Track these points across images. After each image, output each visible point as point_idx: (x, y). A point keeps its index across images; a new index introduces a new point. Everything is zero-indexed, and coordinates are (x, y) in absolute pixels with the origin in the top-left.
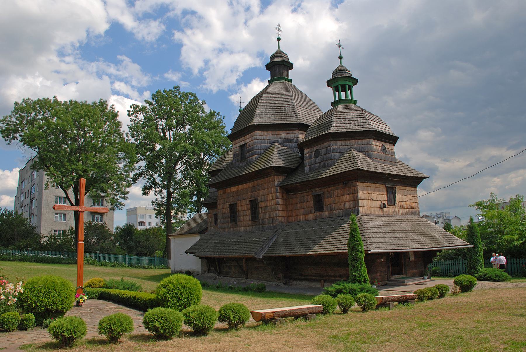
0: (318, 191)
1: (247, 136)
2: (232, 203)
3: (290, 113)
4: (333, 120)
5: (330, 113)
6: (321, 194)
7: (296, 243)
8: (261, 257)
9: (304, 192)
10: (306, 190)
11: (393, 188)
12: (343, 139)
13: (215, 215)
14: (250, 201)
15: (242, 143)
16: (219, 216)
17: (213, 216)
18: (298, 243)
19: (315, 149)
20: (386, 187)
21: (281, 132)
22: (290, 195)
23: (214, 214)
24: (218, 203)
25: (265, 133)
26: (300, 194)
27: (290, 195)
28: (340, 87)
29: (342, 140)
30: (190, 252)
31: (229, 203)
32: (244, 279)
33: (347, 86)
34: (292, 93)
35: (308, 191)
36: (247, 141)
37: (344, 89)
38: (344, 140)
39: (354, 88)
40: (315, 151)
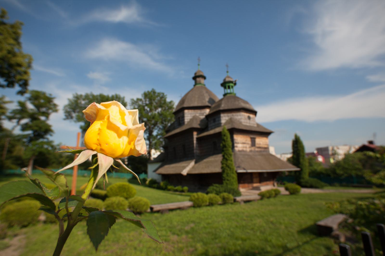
5: (221, 100)
34: (204, 91)
37: (229, 87)
39: (235, 88)
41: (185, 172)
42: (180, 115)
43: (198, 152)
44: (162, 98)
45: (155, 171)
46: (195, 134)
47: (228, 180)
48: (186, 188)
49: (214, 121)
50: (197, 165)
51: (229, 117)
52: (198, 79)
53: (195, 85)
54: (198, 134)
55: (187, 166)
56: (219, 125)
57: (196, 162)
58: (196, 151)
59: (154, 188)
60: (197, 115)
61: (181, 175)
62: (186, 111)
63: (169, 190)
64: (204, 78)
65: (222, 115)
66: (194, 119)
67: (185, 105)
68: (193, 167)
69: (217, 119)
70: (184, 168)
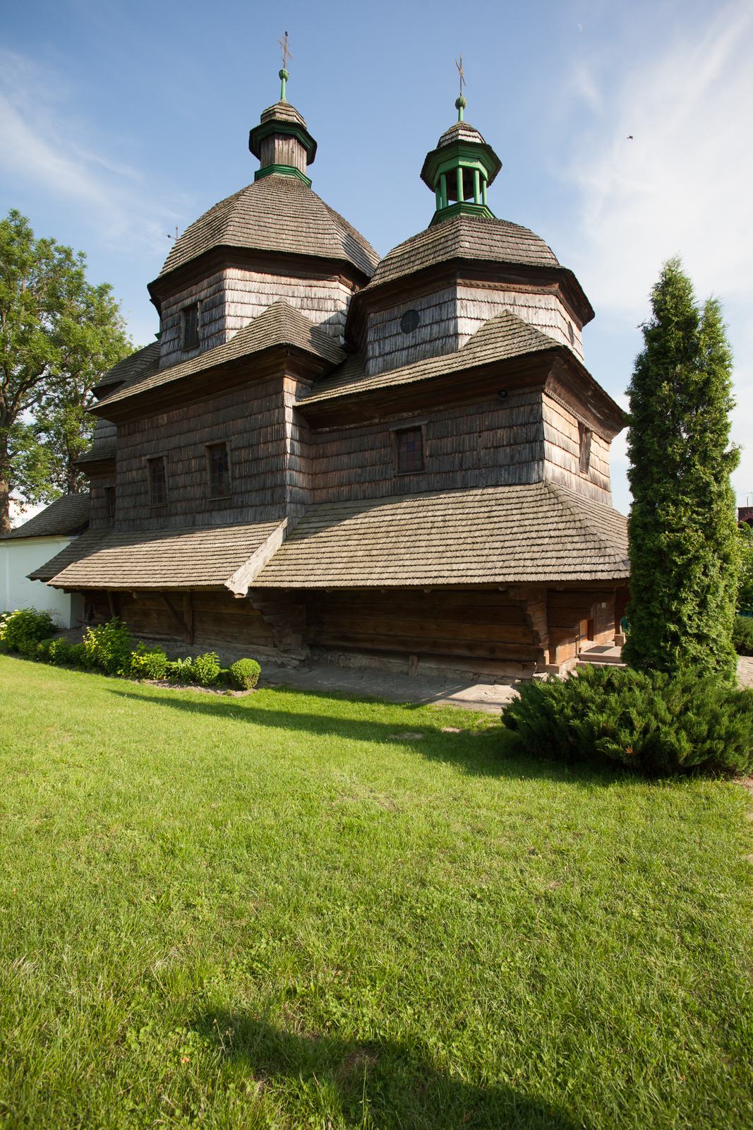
0: (407, 420)
1: (205, 283)
2: (155, 456)
3: (320, 236)
4: (462, 232)
6: (419, 429)
7: (351, 554)
8: (245, 591)
9: (365, 423)
10: (375, 418)
11: (587, 430)
12: (486, 283)
13: (110, 491)
14: (207, 447)
15: (188, 302)
16: (118, 491)
17: (103, 493)
18: (360, 553)
19: (403, 309)
20: (580, 423)
21: (294, 281)
22: (320, 433)
23: (108, 489)
24: (118, 458)
25: (255, 275)
26: (349, 429)
27: (320, 433)
28: (461, 170)
29: (484, 287)
30: (42, 576)
31: (148, 457)
32: (184, 644)
33: (477, 174)
35: (377, 421)
36: (203, 294)
38: (490, 288)
40: (404, 316)
41: (240, 584)
42: (201, 291)
43: (300, 479)
44: (58, 269)
45: (42, 575)
46: (290, 385)
47: (701, 638)
48: (248, 666)
49: (410, 322)
50: (293, 547)
51: (500, 310)
52: (279, 145)
53: (259, 176)
54: (299, 397)
55: (252, 549)
56: (446, 340)
57: (289, 537)
58: (296, 478)
59: (44, 658)
60: (293, 302)
61: (222, 594)
62: (233, 275)
63: (142, 674)
64: (310, 148)
65: (461, 292)
66: (277, 313)
67: (233, 237)
68: (279, 557)
69: (426, 317)
70: (237, 558)
